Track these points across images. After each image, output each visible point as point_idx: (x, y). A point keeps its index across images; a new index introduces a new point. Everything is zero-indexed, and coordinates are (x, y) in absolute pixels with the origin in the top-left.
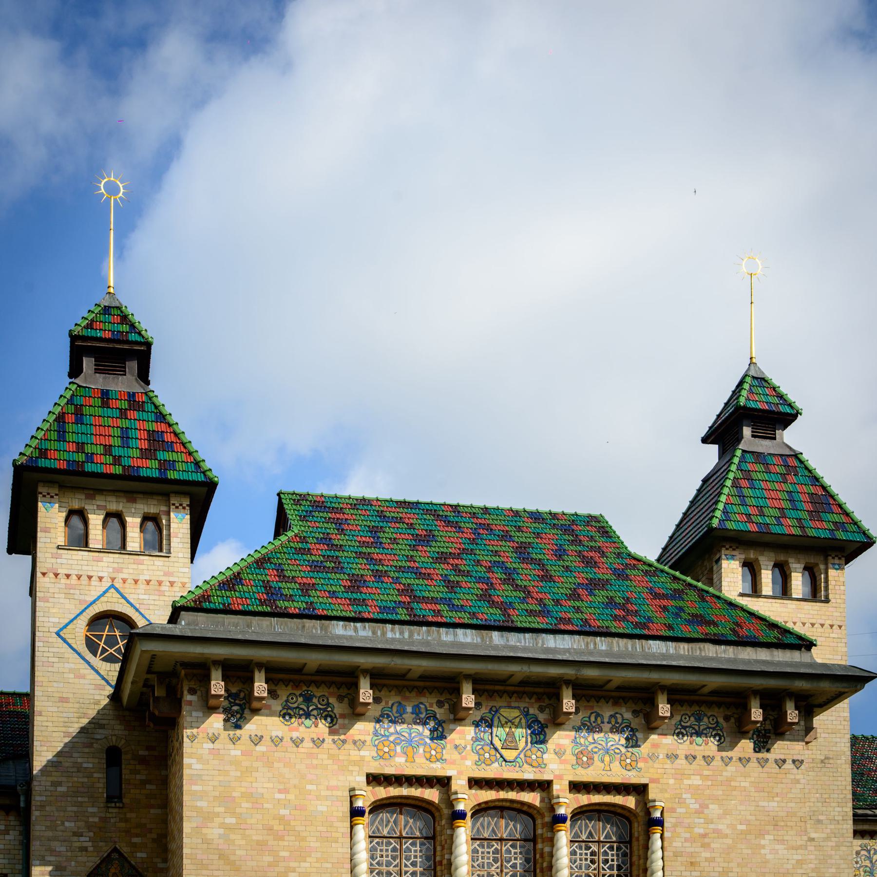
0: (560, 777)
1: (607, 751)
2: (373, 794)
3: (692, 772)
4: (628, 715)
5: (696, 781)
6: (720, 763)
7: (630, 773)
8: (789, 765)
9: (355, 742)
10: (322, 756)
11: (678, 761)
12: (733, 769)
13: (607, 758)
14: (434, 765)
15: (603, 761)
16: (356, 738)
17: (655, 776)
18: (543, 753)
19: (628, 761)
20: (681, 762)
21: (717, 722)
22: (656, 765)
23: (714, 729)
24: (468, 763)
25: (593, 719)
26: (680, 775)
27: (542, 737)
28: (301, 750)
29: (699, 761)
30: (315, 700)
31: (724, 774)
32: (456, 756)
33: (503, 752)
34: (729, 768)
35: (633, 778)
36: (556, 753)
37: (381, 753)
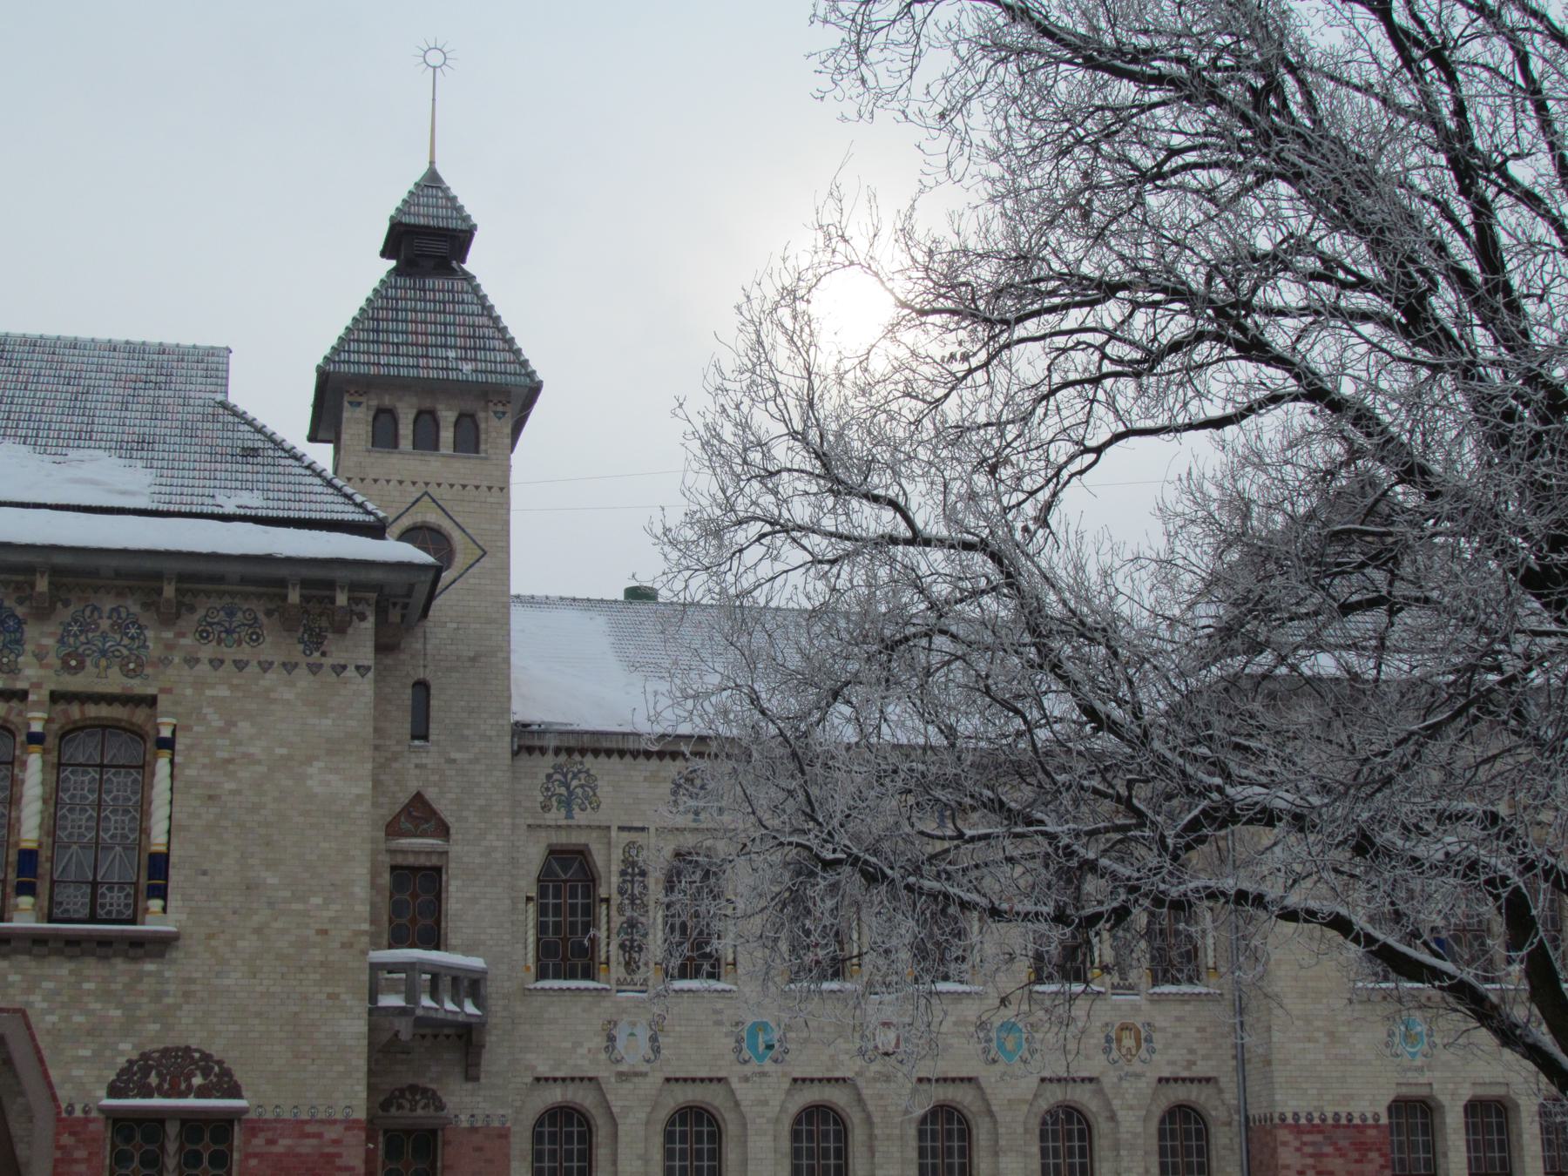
0: (38, 685)
1: (103, 653)
4: (135, 609)
5: (223, 692)
6: (257, 669)
7: (133, 682)
8: (350, 672)
11: (198, 667)
12: (274, 676)
13: (103, 662)
15: (97, 666)
17: (168, 685)
18: (18, 656)
19: (132, 666)
20: (203, 668)
21: (256, 618)
23: (250, 626)
25: (87, 613)
26: (200, 684)
34: (268, 675)
35: (138, 687)
36: (35, 656)
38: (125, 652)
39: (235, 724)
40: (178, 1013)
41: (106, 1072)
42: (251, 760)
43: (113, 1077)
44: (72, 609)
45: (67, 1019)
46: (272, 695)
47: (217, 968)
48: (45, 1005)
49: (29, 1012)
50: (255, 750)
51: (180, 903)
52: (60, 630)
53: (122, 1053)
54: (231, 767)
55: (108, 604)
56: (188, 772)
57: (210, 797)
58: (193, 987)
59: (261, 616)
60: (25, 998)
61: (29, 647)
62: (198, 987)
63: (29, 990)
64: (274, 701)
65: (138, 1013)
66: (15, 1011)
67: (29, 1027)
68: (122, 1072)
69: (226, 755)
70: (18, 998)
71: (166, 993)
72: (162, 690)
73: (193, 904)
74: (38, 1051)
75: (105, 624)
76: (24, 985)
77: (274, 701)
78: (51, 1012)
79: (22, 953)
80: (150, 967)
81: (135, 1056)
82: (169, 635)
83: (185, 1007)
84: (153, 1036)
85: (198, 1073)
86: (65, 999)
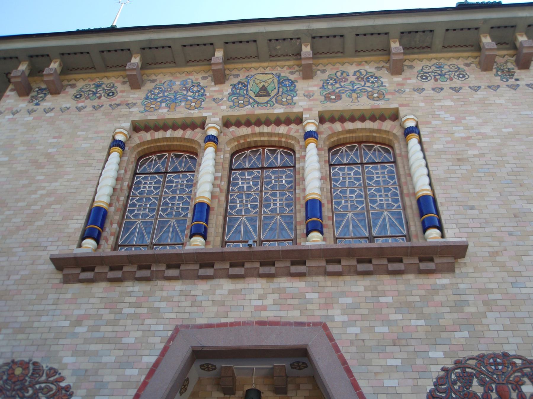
0: (309, 110)
2: (139, 138)
3: (442, 98)
5: (448, 103)
9: (127, 105)
10: (98, 114)
14: (192, 112)
16: (129, 102)
18: (294, 96)
20: (429, 92)
22: (404, 95)
24: (224, 107)
27: (292, 88)
28: (81, 113)
29: (447, 91)
30: (104, 86)
31: (475, 96)
32: (214, 104)
33: (256, 98)
37: (147, 109)
38: (369, 89)
39: (464, 118)
40: (484, 321)
41: (420, 382)
42: (485, 137)
43: (430, 387)
44: (327, 73)
45: (370, 330)
46: (486, 102)
47: (513, 280)
48: (345, 318)
49: (329, 324)
50: (487, 130)
51: (457, 231)
52: (322, 83)
53: (436, 361)
54: (470, 142)
55: (351, 69)
56: (435, 146)
57: (459, 160)
58: (491, 297)
59: (462, 66)
60: (324, 312)
61: (300, 92)
62: (499, 297)
63: (328, 305)
64: (490, 105)
65: (442, 322)
66: (315, 324)
67: (331, 338)
68: (438, 383)
69: (463, 135)
70: (317, 313)
71: (466, 303)
72: (402, 105)
73: (470, 230)
74: (344, 362)
75: (352, 78)
76: (323, 301)
77: (490, 105)
78: (351, 323)
79: (317, 274)
80: (442, 280)
81: (449, 364)
82: (398, 79)
83: (489, 315)
84: (464, 344)
85: (525, 379)
86: (365, 312)
